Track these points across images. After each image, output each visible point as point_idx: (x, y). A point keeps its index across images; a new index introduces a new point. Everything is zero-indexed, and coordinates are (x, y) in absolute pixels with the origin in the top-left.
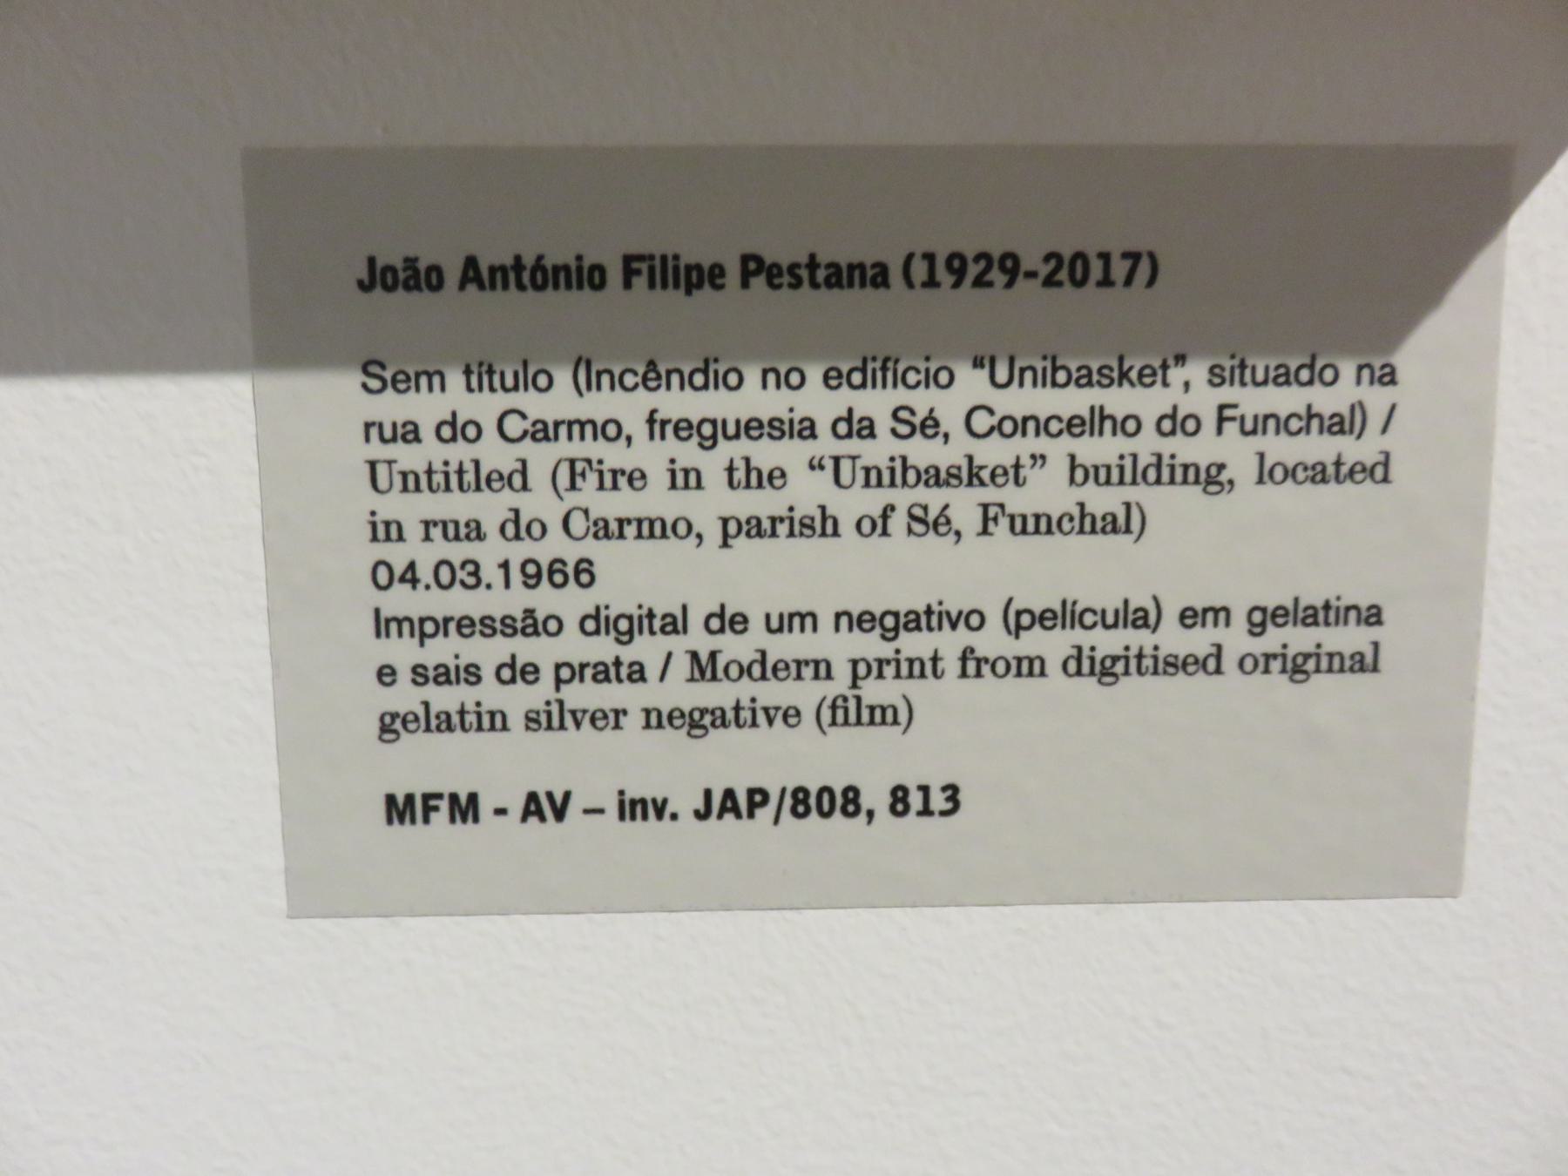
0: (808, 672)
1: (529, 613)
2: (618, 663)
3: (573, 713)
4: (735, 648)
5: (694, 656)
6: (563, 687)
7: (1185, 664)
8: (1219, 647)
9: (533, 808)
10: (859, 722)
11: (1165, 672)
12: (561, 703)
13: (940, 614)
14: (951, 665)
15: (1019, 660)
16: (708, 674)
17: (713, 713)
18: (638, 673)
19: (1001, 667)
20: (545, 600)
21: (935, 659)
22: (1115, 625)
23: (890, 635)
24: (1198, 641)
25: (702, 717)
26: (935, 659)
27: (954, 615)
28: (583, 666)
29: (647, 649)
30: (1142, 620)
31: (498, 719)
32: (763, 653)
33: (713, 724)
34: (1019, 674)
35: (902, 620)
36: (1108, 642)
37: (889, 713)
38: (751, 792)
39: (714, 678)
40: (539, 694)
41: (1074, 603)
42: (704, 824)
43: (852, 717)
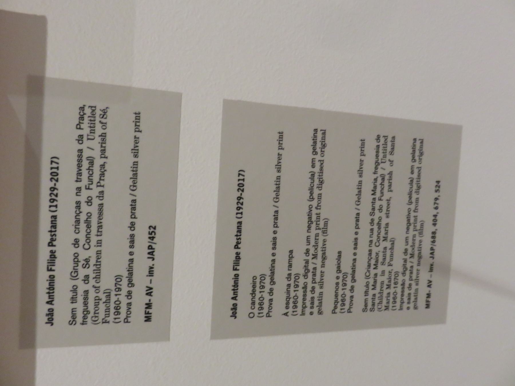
7: (321, 167)
8: (319, 161)
10: (327, 228)
11: (323, 171)
14: (318, 211)
15: (318, 199)
19: (319, 202)
22: (314, 180)
24: (318, 164)
26: (317, 214)
30: (313, 175)
34: (321, 198)
35: (310, 220)
36: (317, 182)
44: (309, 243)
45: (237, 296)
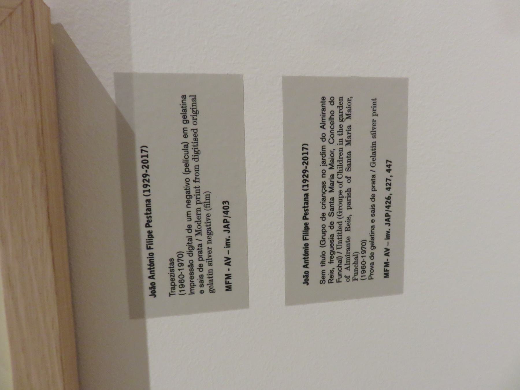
0: (199, 213)
1: (189, 266)
2: (198, 249)
3: (209, 257)
4: (195, 227)
5: (196, 235)
6: (203, 259)
9: (228, 264)
12: (207, 259)
13: (186, 187)
14: (197, 184)
15: (195, 171)
16: (200, 232)
17: (208, 231)
18: (200, 245)
19: (197, 174)
20: (186, 263)
21: (196, 188)
23: (191, 197)
25: (209, 233)
27: (187, 184)
28: (199, 256)
29: (195, 244)
31: (210, 271)
32: (195, 221)
33: (210, 230)
34: (198, 171)
35: (188, 195)
37: (207, 196)
38: (224, 222)
39: (201, 231)
40: (205, 264)
41: (183, 160)
42: (231, 232)
43: (208, 203)
44: (191, 218)
45: (154, 275)
